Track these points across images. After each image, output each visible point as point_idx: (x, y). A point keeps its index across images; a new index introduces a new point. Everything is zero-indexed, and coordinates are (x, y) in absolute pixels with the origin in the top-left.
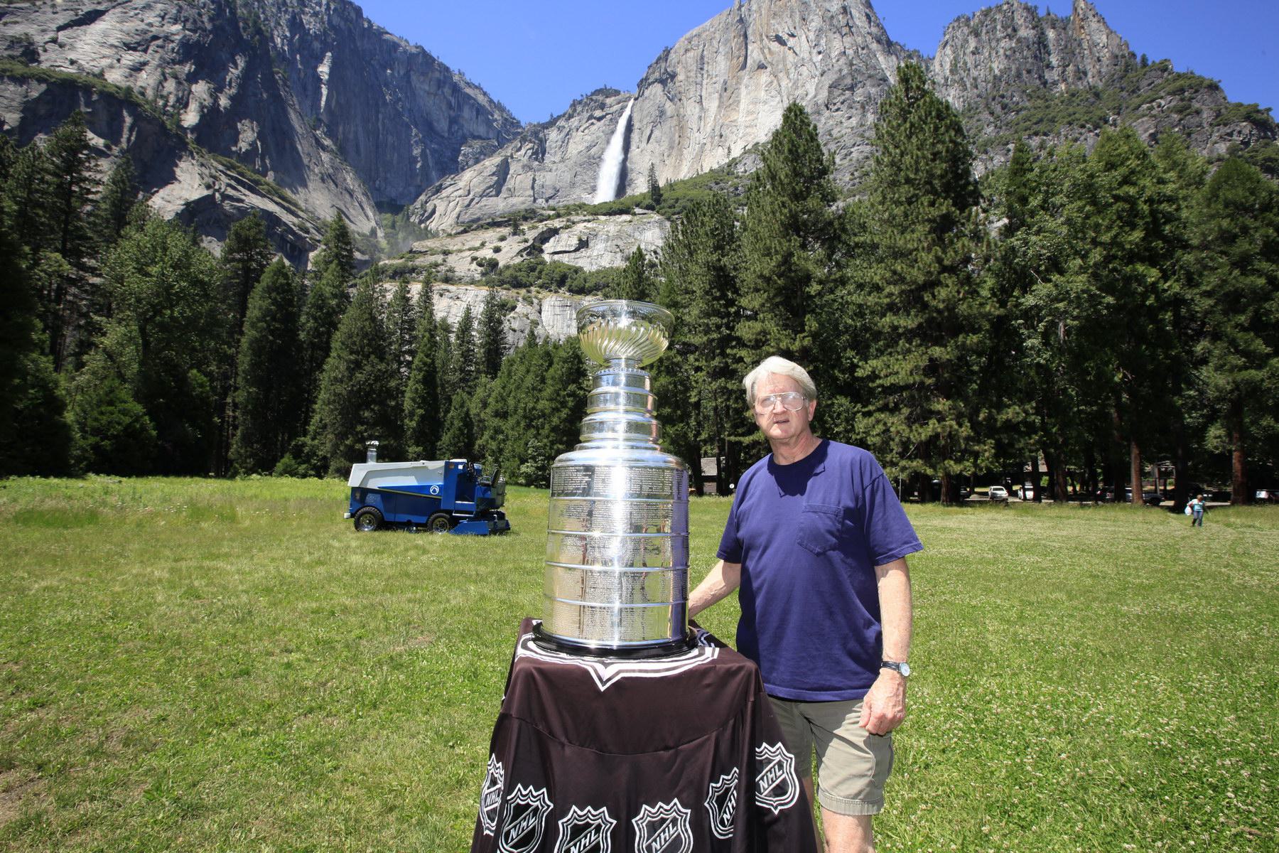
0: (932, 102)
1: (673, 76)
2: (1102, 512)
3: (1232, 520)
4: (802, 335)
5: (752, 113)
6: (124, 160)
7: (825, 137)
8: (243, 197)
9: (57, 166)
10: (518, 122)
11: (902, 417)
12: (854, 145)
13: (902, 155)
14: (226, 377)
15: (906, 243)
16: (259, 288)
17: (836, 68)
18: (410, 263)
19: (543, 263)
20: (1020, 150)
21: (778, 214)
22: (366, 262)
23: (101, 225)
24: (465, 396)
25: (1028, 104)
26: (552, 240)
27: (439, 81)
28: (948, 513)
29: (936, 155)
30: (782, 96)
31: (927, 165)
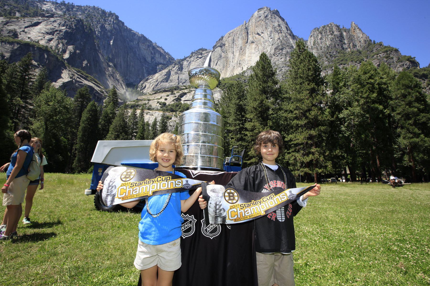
1: (224, 45)
2: (368, 185)
5: (250, 57)
6: (44, 69)
8: (82, 81)
9: (21, 70)
10: (174, 59)
11: (301, 154)
13: (298, 69)
14: (73, 140)
15: (300, 97)
16: (86, 110)
17: (277, 43)
18: (137, 103)
19: (181, 104)
20: (336, 68)
21: (258, 88)
23: (34, 89)
25: (338, 55)
26: (184, 96)
27: (148, 46)
29: (309, 69)
30: (259, 52)
31: (306, 72)
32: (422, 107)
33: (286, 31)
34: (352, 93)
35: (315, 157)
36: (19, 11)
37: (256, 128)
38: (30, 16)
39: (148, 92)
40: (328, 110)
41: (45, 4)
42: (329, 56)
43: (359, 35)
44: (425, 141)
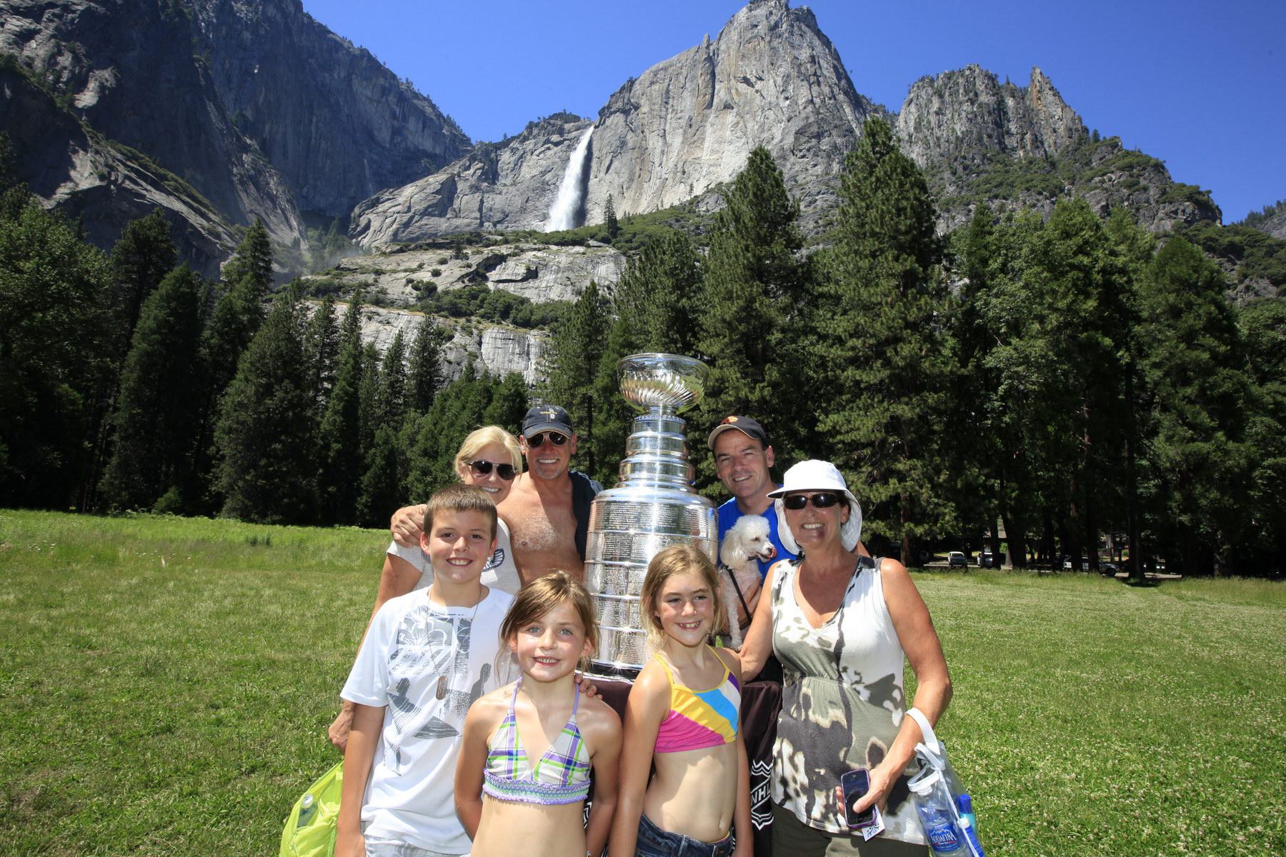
1: (637, 107)
3: (1184, 592)
4: (762, 385)
5: (717, 152)
8: (144, 192)
10: (469, 140)
11: (864, 476)
12: (819, 193)
13: (867, 209)
15: (870, 295)
16: (155, 295)
17: (803, 115)
18: (336, 281)
19: (487, 291)
20: (983, 211)
21: (741, 258)
22: (285, 275)
24: (390, 431)
25: (988, 168)
26: (498, 267)
29: (900, 211)
30: (747, 138)
31: (892, 219)
32: (1223, 349)
35: (905, 489)
40: (951, 342)
42: (960, 169)
44: (1227, 453)
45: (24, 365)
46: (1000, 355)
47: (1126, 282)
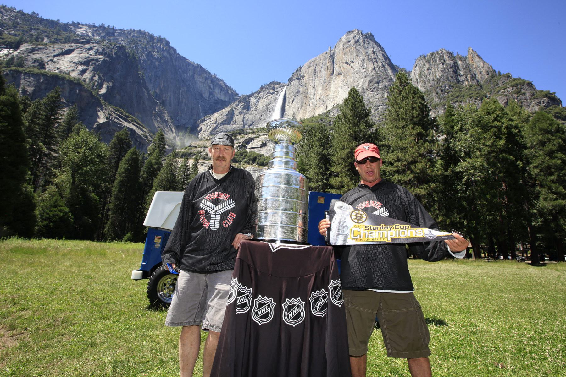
0: (411, 87)
1: (303, 77)
5: (336, 92)
7: (367, 102)
10: (238, 94)
12: (379, 105)
13: (400, 108)
14: (106, 198)
15: (403, 144)
16: (124, 159)
19: (247, 152)
23: (60, 132)
28: (427, 264)
31: (410, 112)
33: (384, 60)
34: (470, 139)
36: (47, 36)
37: (344, 186)
38: (61, 43)
39: (203, 137)
40: (440, 162)
41: (81, 28)
42: (440, 92)
43: (478, 64)
45: (79, 187)
46: (462, 166)
47: (518, 132)
